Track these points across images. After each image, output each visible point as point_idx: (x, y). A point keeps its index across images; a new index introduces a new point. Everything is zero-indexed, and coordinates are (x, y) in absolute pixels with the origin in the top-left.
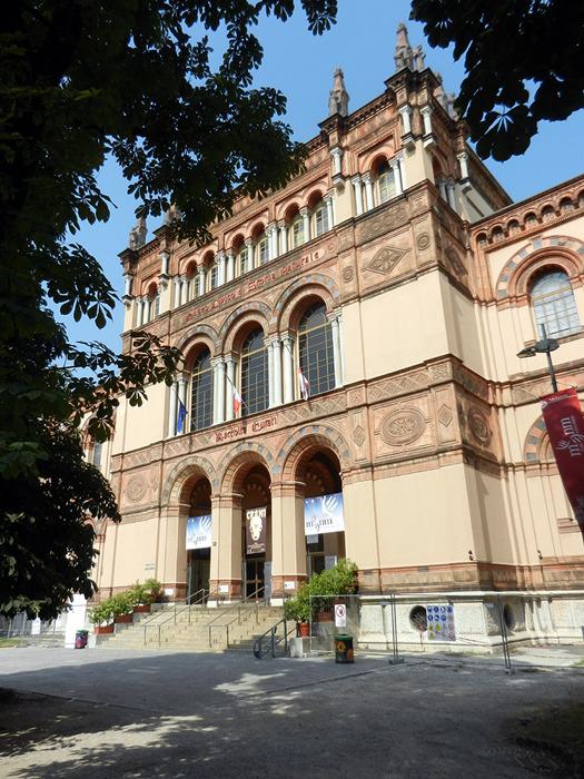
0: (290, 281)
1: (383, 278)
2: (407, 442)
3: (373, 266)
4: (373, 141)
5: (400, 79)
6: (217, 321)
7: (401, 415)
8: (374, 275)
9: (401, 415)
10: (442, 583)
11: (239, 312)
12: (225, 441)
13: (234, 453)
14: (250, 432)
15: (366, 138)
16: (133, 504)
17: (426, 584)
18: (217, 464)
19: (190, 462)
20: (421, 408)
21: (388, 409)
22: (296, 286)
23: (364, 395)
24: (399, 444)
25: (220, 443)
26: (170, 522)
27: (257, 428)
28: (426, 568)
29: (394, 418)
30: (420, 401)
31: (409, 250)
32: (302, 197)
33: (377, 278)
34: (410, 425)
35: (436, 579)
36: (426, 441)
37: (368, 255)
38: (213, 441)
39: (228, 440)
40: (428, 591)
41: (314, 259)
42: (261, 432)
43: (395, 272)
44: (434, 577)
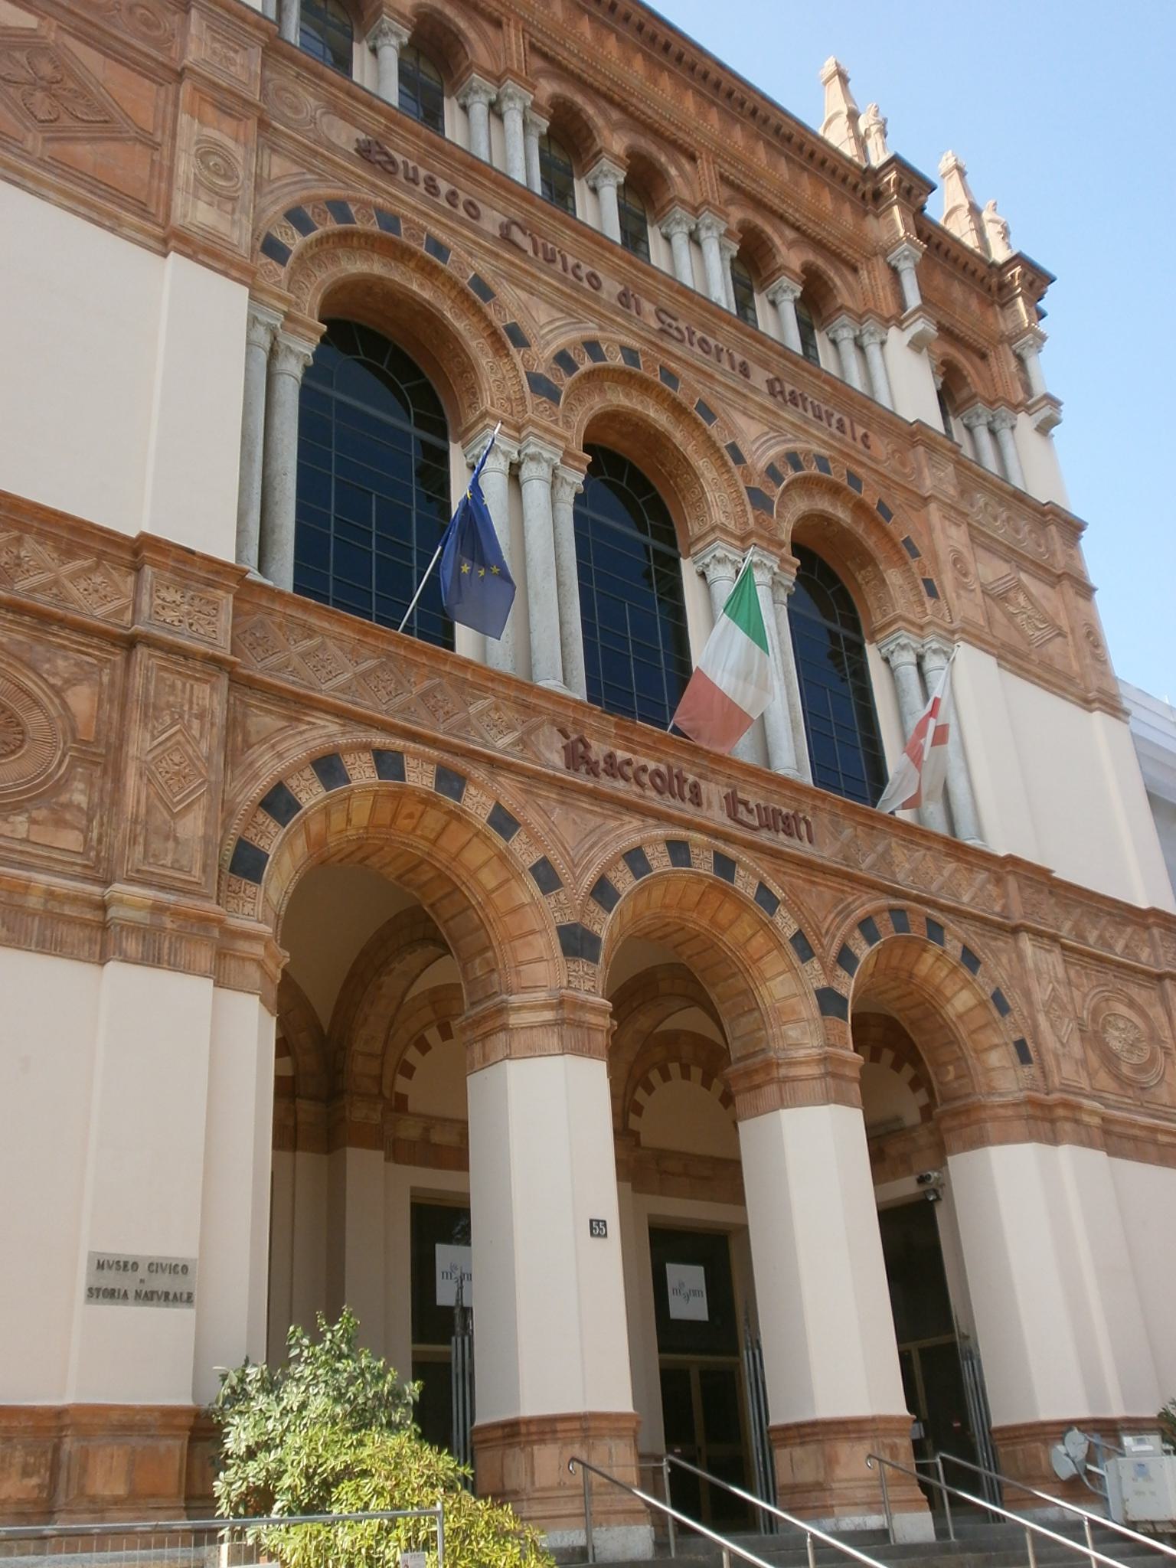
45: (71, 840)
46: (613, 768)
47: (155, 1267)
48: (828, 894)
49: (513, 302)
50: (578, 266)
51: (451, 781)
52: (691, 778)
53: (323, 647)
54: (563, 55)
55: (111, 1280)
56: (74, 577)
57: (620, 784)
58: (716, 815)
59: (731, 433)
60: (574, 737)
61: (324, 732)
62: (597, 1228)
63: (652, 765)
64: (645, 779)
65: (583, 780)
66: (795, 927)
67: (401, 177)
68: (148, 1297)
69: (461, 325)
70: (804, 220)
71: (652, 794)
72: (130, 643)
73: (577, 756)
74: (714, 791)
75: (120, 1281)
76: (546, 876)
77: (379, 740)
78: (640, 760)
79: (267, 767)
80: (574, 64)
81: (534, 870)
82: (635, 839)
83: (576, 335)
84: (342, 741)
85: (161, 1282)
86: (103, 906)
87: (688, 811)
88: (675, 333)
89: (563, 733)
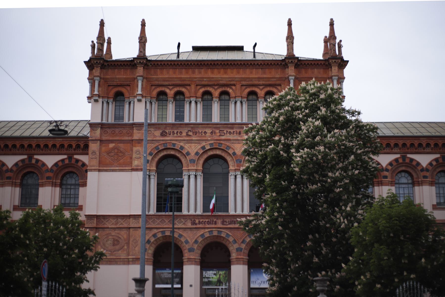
5: (337, 61)
6: (193, 149)
12: (198, 226)
13: (207, 235)
14: (219, 225)
18: (191, 240)
19: (168, 233)
25: (194, 226)
27: (225, 223)
32: (261, 90)
38: (189, 225)
39: (201, 226)
42: (229, 226)
45: (125, 252)
46: (200, 223)
48: (242, 232)
49: (187, 147)
50: (202, 132)
51: (173, 232)
52: (215, 220)
54: (204, 83)
56: (124, 222)
57: (201, 225)
58: (219, 225)
59: (234, 150)
60: (193, 220)
61: (155, 231)
62: (191, 286)
63: (207, 220)
64: (206, 223)
65: (194, 226)
66: (233, 239)
67: (168, 135)
69: (178, 155)
70: (265, 82)
72: (130, 228)
73: (194, 223)
74: (219, 221)
76: (187, 242)
77: (161, 230)
78: (204, 220)
79: (147, 238)
80: (206, 83)
81: (185, 242)
82: (202, 233)
83: (200, 147)
84: (156, 232)
86: (128, 259)
87: (213, 226)
88: (223, 134)
89: (191, 220)
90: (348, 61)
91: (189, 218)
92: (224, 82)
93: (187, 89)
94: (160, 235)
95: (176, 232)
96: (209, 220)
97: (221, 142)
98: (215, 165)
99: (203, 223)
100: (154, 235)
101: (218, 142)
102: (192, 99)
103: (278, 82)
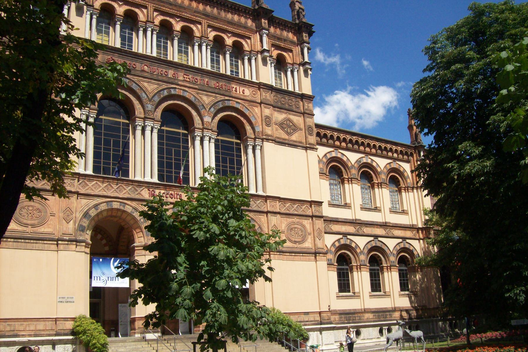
0: (223, 98)
1: (286, 137)
2: (299, 243)
3: (281, 125)
4: (282, 45)
7: (296, 226)
8: (281, 131)
9: (296, 226)
10: (315, 321)
11: (173, 92)
15: (279, 39)
16: (20, 228)
17: (307, 321)
20: (306, 225)
21: (290, 220)
22: (227, 104)
23: (277, 206)
24: (295, 242)
26: (78, 258)
28: (307, 313)
29: (293, 226)
30: (306, 221)
31: (301, 130)
32: (229, 37)
33: (283, 135)
34: (300, 233)
35: (312, 319)
36: (308, 244)
37: (279, 116)
40: (309, 325)
41: (241, 93)
43: (295, 137)
44: (311, 318)
47: (68, 298)
53: (97, 183)
55: (61, 300)
68: (67, 302)
71: (170, 199)
75: (62, 300)
84: (100, 201)
85: (69, 300)
90: (314, 32)
91: (146, 187)
92: (188, 15)
93: (142, 12)
94: (103, 207)
95: (128, 205)
96: (173, 192)
97: (186, 89)
98: (177, 119)
99: (164, 195)
100: (96, 206)
101: (182, 88)
102: (149, 24)
103: (247, 34)
